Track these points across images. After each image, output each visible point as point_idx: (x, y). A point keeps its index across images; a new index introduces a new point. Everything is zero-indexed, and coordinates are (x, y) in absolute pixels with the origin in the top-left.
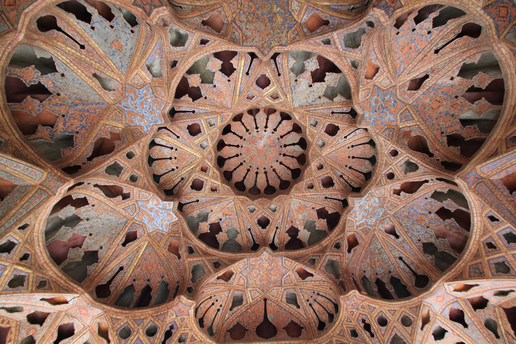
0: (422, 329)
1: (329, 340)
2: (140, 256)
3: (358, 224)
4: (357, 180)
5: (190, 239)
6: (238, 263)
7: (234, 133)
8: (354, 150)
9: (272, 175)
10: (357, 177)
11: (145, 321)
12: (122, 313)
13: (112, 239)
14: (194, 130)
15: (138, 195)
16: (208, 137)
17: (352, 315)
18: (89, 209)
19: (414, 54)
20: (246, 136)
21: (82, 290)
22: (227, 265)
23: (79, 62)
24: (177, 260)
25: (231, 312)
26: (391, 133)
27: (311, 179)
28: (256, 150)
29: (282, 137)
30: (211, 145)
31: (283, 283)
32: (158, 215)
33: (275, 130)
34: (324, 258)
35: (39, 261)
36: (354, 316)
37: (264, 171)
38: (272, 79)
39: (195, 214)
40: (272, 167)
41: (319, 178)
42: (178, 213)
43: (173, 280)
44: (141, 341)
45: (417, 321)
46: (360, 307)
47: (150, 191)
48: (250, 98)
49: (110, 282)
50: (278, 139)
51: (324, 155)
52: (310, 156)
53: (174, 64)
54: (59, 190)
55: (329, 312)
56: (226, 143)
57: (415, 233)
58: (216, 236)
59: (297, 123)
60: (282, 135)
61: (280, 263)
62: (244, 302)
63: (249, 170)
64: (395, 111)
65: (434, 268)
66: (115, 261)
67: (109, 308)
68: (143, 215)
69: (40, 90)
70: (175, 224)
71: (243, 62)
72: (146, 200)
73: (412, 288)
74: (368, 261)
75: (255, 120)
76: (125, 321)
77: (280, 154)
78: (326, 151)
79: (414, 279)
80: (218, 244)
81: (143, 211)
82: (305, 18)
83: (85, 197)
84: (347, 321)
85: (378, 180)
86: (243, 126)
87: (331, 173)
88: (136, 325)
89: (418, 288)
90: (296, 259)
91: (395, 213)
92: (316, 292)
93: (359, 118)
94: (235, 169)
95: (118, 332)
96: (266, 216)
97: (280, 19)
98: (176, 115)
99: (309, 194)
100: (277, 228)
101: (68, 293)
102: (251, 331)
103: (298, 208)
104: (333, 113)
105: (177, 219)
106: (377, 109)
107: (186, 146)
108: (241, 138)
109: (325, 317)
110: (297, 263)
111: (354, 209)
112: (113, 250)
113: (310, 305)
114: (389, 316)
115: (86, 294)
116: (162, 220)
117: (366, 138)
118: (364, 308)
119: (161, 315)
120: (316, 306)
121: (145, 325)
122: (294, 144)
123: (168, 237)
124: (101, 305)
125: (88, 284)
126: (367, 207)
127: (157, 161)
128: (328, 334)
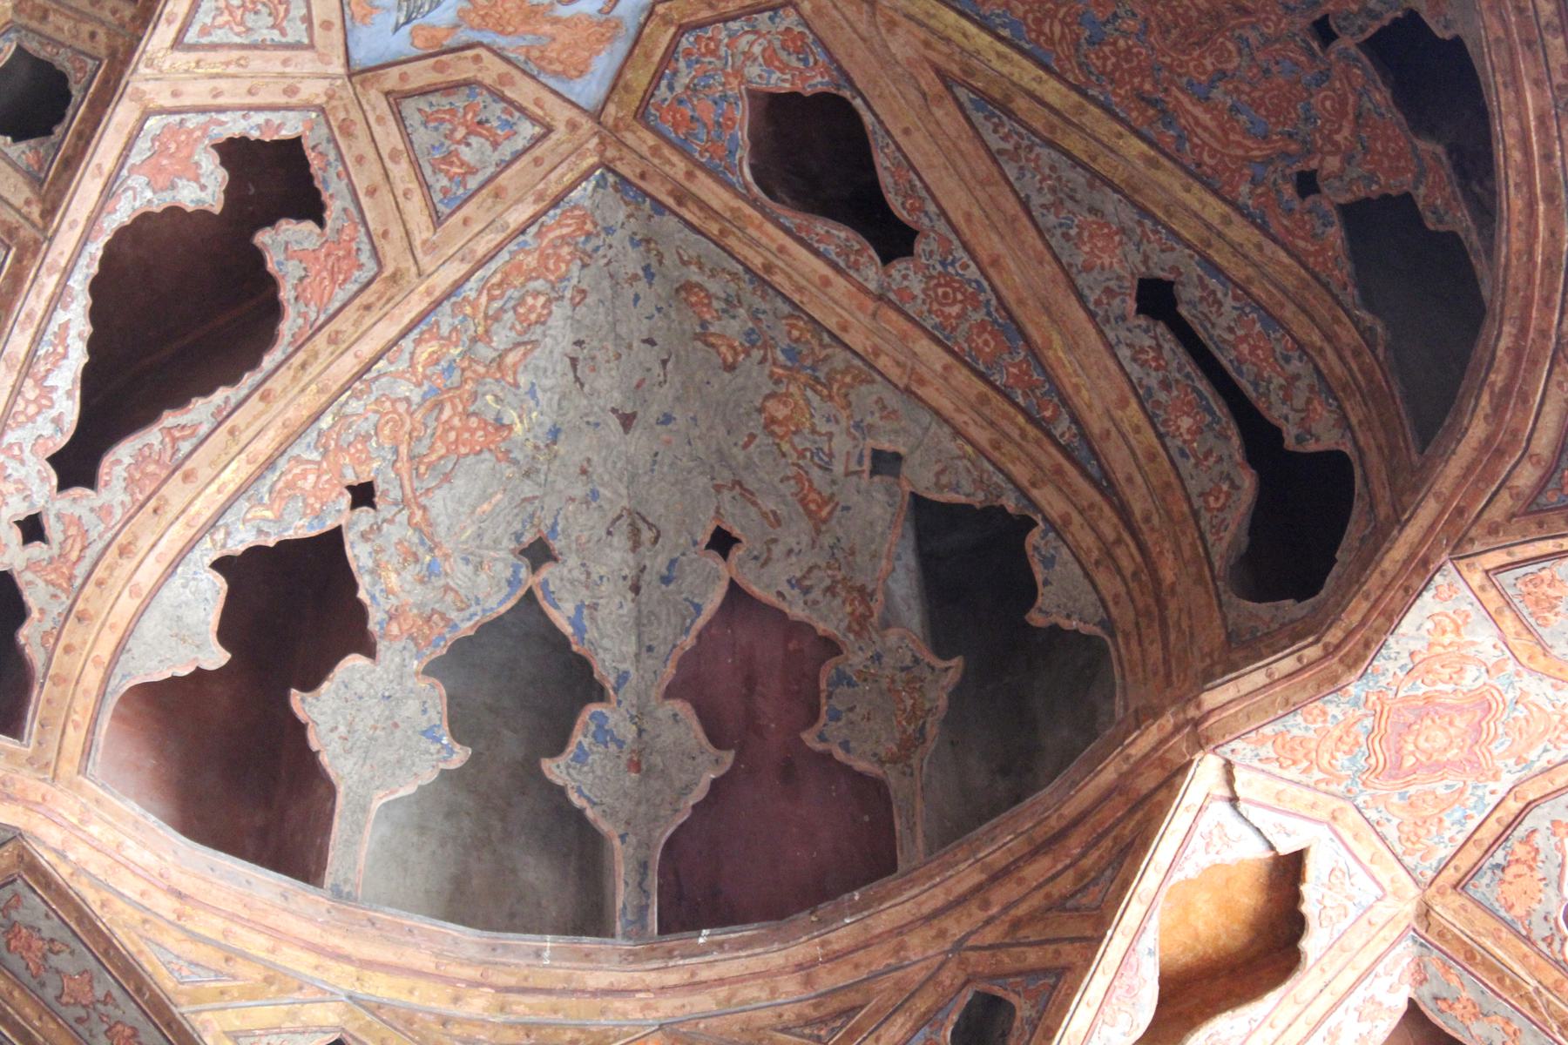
2: (1053, 91)
13: (813, 354)
18: (398, 532)
21: (1168, 721)
35: (765, 1017)
49: (1260, 438)
66: (1057, 353)
83: (221, 565)
101: (1145, 846)
115: (1211, 699)
124: (1373, 582)
125: (1155, 652)
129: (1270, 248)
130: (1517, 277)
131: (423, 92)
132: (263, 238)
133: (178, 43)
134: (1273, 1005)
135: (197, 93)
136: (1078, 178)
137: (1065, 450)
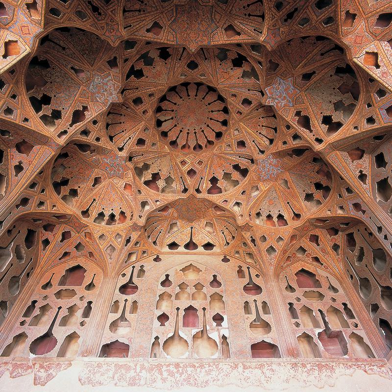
7: (213, 130)
11: (308, 29)
12: (327, 35)
14: (242, 144)
16: (233, 135)
17: (111, 19)
19: (106, 197)
20: (203, 126)
23: (294, 196)
29: (176, 126)
33: (181, 131)
38: (186, 175)
40: (183, 100)
48: (200, 163)
53: (243, 192)
54: (325, 146)
58: (237, 57)
61: (178, 36)
63: (203, 99)
69: (318, 186)
71: (204, 186)
72: (286, 107)
74: (95, 46)
75: (197, 140)
78: (141, 126)
82: (170, 211)
85: (102, 117)
94: (215, 101)
96: (190, 70)
97: (184, 209)
100: (180, 59)
103: (160, 77)
105: (266, 89)
108: (208, 126)
110: (162, 41)
118: (101, 27)
122: (165, 121)
134: (379, 56)
135: (291, 117)
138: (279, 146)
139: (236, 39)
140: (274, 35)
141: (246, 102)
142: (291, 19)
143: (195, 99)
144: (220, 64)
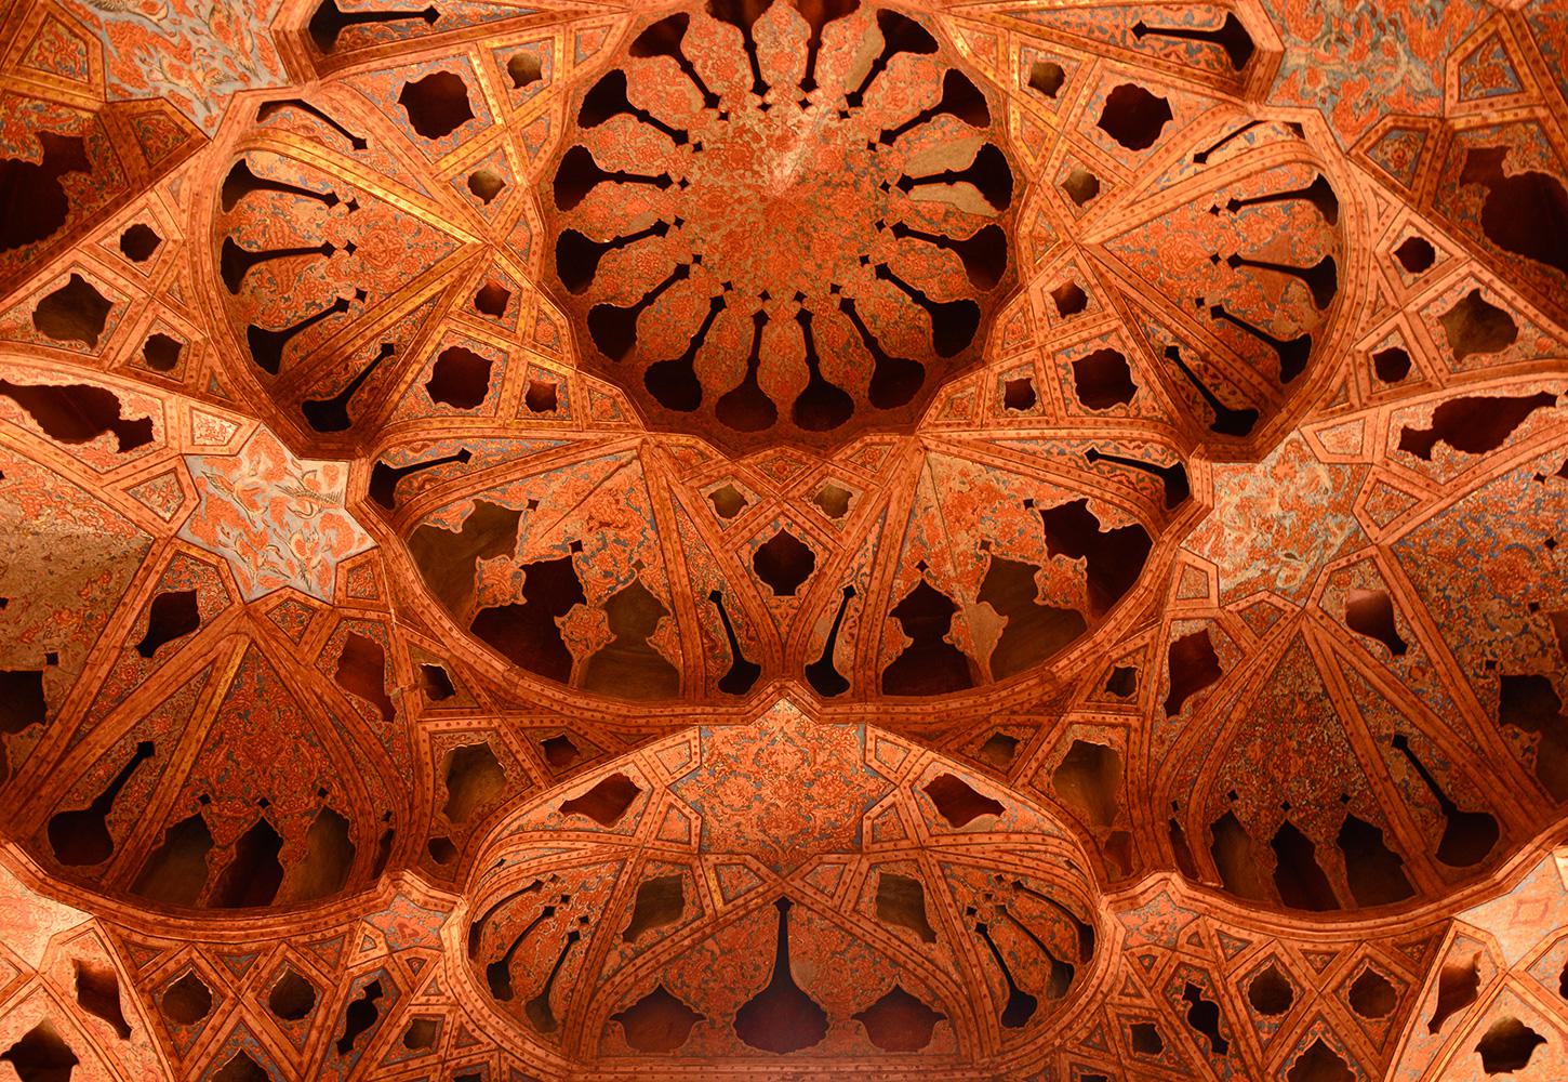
0: (1434, 1026)
1: (1042, 1064)
2: (217, 701)
3: (1226, 584)
4: (1247, 373)
5: (433, 636)
6: (656, 746)
7: (644, 116)
8: (1241, 224)
9: (833, 330)
10: (1248, 362)
11: (262, 960)
12: (169, 929)
13: (92, 626)
14: (437, 107)
15: (186, 431)
17: (1148, 969)
20: (708, 129)
22: (604, 756)
24: (379, 727)
25: (629, 949)
26: (1410, 155)
27: (1026, 357)
28: (755, 203)
29: (888, 137)
30: (522, 175)
31: (866, 839)
32: (286, 521)
33: (855, 99)
34: (1054, 736)
36: (1153, 974)
37: (796, 308)
39: (453, 516)
40: (835, 289)
41: (1061, 358)
42: (372, 516)
43: (368, 807)
44: (253, 1034)
45: (1415, 996)
46: (1183, 940)
47: (239, 410)
49: (104, 803)
50: (871, 146)
51: (1092, 239)
52: (1024, 244)
55: (1056, 956)
56: (600, 165)
57: (1478, 634)
58: (558, 621)
59: (962, 69)
60: (888, 126)
61: (854, 755)
62: (689, 912)
63: (718, 304)
64: (1436, 44)
65: (1526, 782)
66: (115, 718)
67: (112, 905)
68: (217, 519)
70: (359, 566)
72: (225, 450)
73: (1424, 863)
74: (1255, 750)
75: (750, 47)
76: (183, 957)
77: (880, 225)
78: (1102, 224)
79: (1437, 830)
80: (567, 659)
81: (214, 502)
84: (1122, 993)
85: (1336, 382)
86: (687, 80)
87: (1125, 332)
88: (228, 976)
89: (1445, 869)
90: (927, 737)
91: (1400, 540)
92: (1010, 877)
93: (1260, 71)
94: (649, 299)
95: (159, 999)
96: (795, 533)
98: (345, 34)
99: (1012, 433)
100: (849, 592)
102: (713, 1022)
104: (1140, 30)
105: (370, 542)
106: (1349, 29)
107: (399, 190)
108: (680, 137)
109: (1035, 978)
110: (930, 754)
111: (1215, 516)
112: (103, 672)
113: (981, 929)
114: (1301, 974)
116: (300, 546)
117: (1297, 168)
118: (1201, 945)
119: (324, 940)
120: (1005, 935)
121: (265, 974)
122: (949, 178)
123: (334, 620)
126: (1275, 510)
127: (262, 266)
128: (1041, 1041)
129: (177, 790)
130: (214, 925)
131: (178, 481)
132: (111, 434)
133: (192, 408)
136: (186, 714)
137: (78, 729)
138: (176, 207)
139: (582, 785)
140: (407, 931)
141: (461, 381)
142: (355, 1004)
143: (765, 296)
144: (639, 565)
